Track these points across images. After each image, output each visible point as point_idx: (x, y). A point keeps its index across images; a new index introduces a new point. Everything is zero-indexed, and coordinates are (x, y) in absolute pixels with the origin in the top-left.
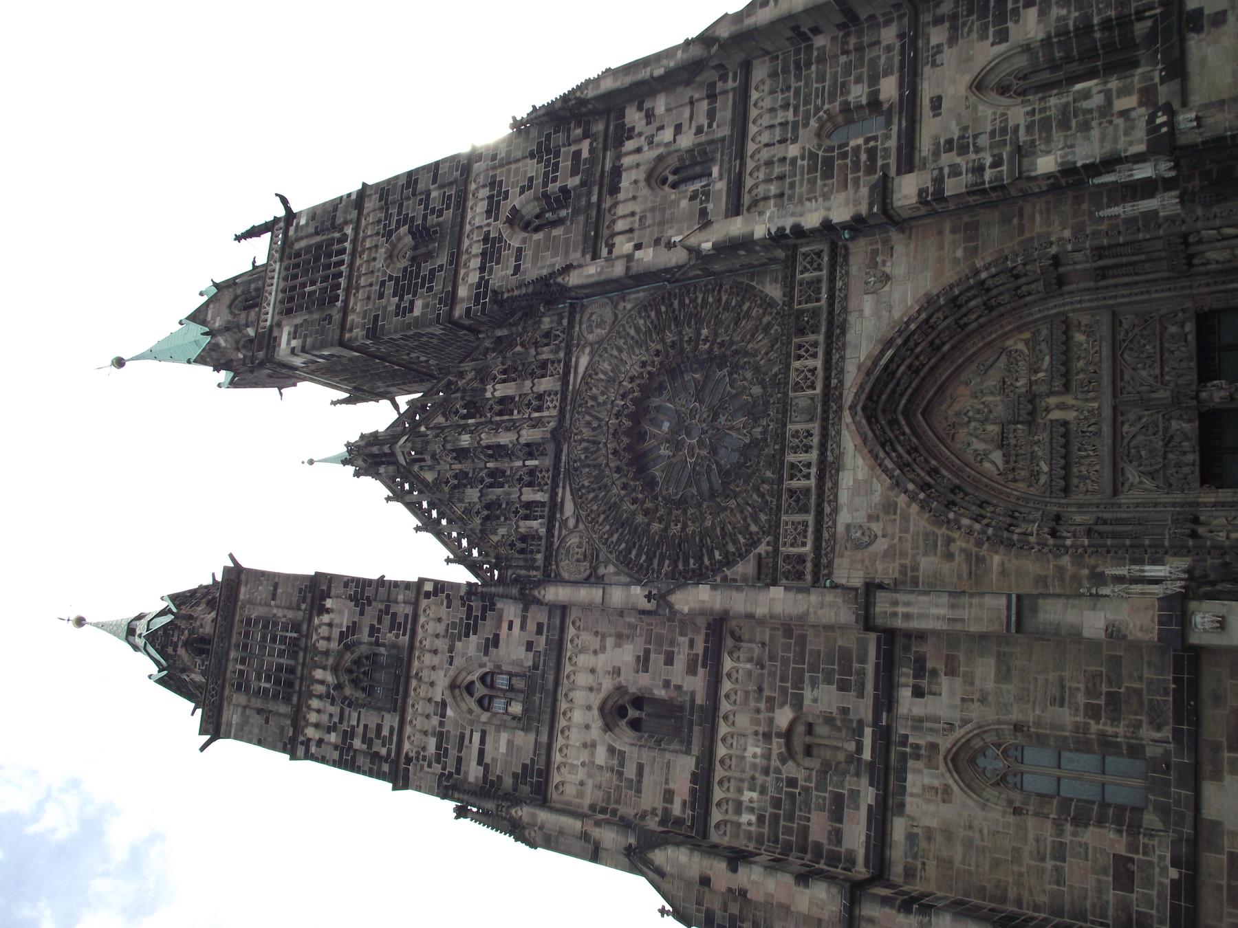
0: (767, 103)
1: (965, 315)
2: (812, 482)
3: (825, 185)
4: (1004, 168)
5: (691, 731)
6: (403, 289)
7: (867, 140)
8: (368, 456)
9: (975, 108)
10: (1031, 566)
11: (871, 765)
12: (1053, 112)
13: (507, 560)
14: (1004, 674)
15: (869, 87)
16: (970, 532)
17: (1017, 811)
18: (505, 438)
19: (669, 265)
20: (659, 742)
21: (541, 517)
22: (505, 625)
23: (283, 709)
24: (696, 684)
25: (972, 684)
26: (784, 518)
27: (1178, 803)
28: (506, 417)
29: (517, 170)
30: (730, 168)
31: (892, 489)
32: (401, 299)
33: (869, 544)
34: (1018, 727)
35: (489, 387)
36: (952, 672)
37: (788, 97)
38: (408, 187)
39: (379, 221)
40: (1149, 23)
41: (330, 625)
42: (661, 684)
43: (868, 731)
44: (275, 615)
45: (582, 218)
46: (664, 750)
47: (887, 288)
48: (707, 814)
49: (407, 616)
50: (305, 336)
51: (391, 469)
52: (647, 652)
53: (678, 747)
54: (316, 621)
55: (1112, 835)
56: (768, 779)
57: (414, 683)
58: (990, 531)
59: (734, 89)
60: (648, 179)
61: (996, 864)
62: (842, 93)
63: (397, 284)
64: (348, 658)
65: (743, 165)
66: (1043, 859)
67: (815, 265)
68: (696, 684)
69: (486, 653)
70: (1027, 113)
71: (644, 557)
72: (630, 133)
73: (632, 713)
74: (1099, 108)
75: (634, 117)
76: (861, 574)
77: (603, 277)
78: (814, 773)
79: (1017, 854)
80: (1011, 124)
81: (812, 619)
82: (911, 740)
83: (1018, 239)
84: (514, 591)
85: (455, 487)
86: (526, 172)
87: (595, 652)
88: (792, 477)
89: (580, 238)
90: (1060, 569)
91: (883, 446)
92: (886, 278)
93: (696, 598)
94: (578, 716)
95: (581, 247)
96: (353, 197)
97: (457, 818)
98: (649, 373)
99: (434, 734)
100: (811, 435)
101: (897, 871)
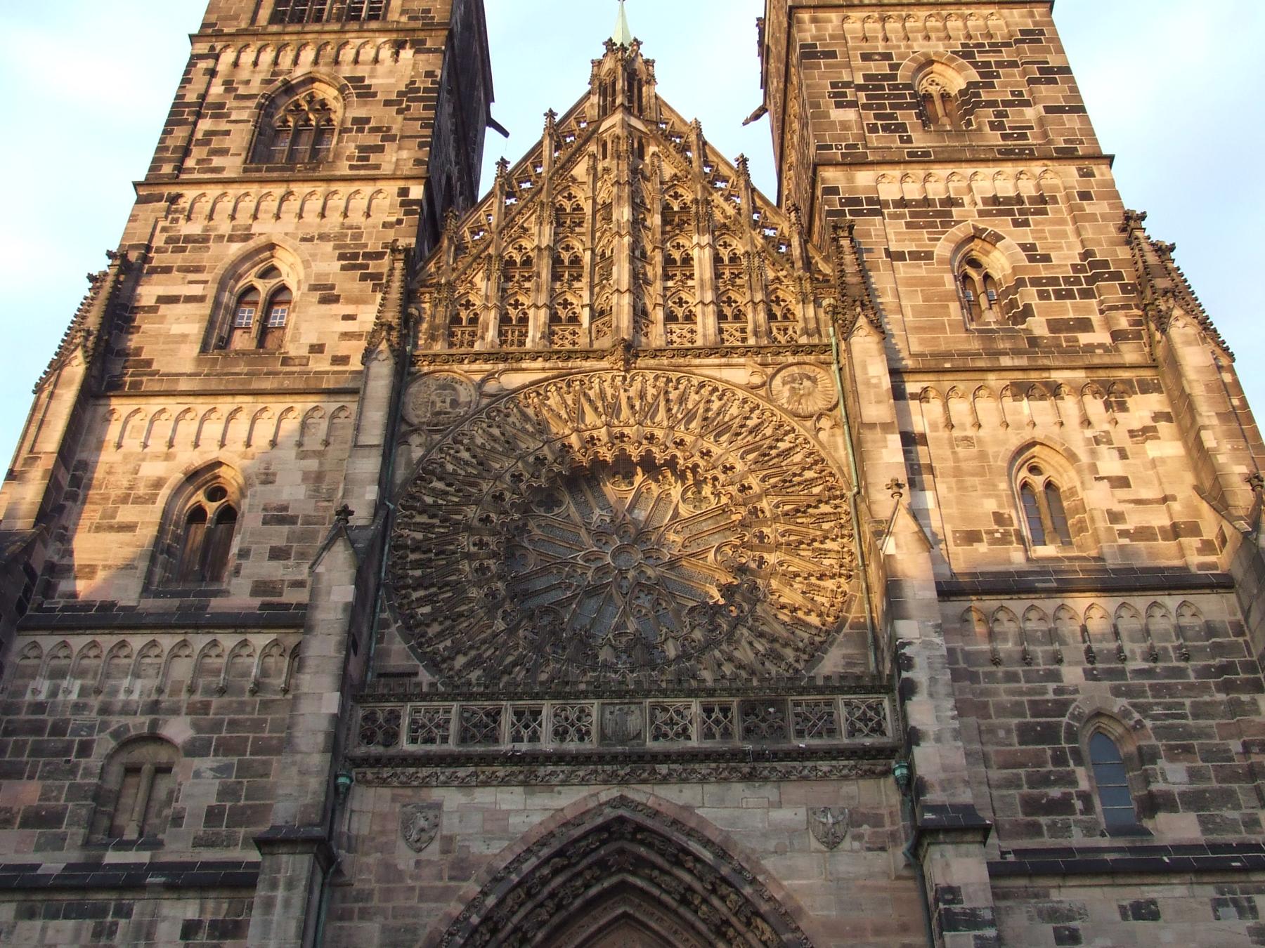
0: (1160, 623)
2: (505, 746)
3: (1008, 731)
5: (174, 595)
6: (876, 88)
7: (1085, 797)
11: (97, 865)
15: (1182, 794)
19: (872, 490)
21: (503, 343)
22: (349, 309)
24: (238, 595)
26: (455, 706)
29: (1064, 235)
31: (489, 871)
32: (860, 88)
35: (706, 239)
38: (1041, 70)
42: (246, 545)
45: (976, 345)
47: (814, 844)
48: (53, 628)
53: (156, 579)
54: (381, 39)
56: (94, 714)
62: (1170, 748)
63: (885, 77)
67: (859, 725)
68: (238, 595)
69: (314, 288)
71: (429, 500)
75: (1143, 408)
76: (365, 831)
77: (861, 388)
78: (95, 780)
82: (122, 922)
84: (392, 316)
86: (1061, 248)
87: (300, 444)
88: (519, 714)
89: (943, 348)
91: (560, 853)
92: (832, 842)
93: (337, 583)
95: (927, 350)
99: (206, 229)
100: (581, 739)
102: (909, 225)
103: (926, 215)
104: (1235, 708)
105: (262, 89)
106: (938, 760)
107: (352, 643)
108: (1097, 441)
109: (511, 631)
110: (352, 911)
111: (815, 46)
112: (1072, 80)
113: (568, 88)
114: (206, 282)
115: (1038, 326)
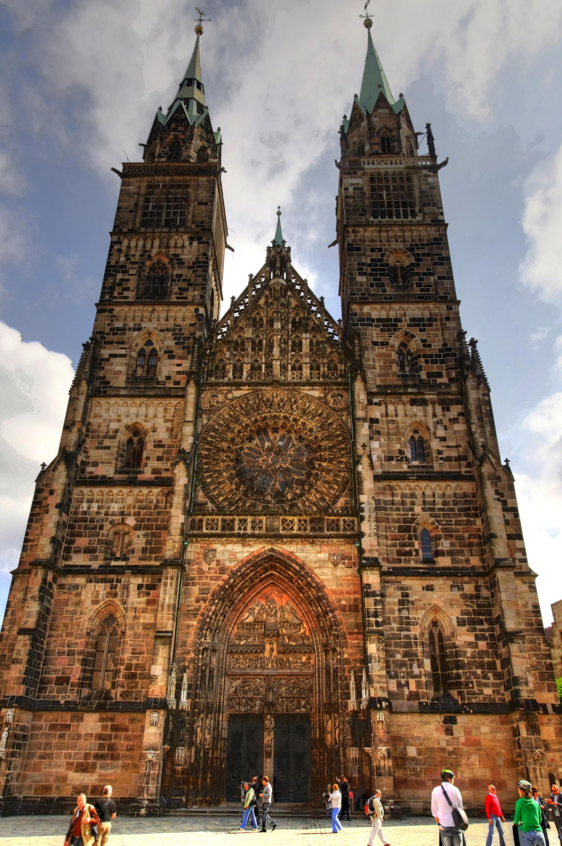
2: (236, 531)
4: (375, 628)
5: (126, 473)
7: (417, 551)
9: (423, 609)
11: (108, 566)
12: (414, 649)
14: (146, 627)
16: (209, 611)
17: (88, 634)
18: (276, 351)
20: (122, 456)
21: (234, 378)
22: (179, 362)
23: (138, 221)
24: (147, 474)
25: (143, 612)
27: (91, 703)
29: (438, 335)
32: (369, 265)
34: (123, 633)
35: (308, 335)
36: (148, 602)
38: (440, 259)
39: (420, 240)
40: (456, 697)
41: (183, 247)
43: (124, 563)
44: (189, 205)
45: (400, 383)
46: (117, 460)
47: (330, 565)
49: (186, 298)
55: (78, 676)
57: (150, 309)
58: (208, 620)
59: (460, 472)
61: (66, 626)
64: (166, 261)
65: (414, 481)
66: (68, 646)
68: (147, 474)
69: (166, 352)
71: (209, 439)
72: (446, 409)
73: (136, 439)
75: (455, 410)
76: (192, 558)
77: (357, 404)
79: (70, 635)
80: (411, 627)
84: (194, 368)
87: (165, 417)
88: (240, 521)
89: (388, 383)
90: (188, 653)
92: (335, 565)
94: (133, 410)
96: (440, 218)
97: (83, 345)
99: (125, 325)
101: (62, 580)
102: (381, 330)
103: (387, 326)
104: (468, 523)
108: (438, 423)
109: (237, 489)
111: (352, 245)
112: (450, 264)
115: (423, 375)
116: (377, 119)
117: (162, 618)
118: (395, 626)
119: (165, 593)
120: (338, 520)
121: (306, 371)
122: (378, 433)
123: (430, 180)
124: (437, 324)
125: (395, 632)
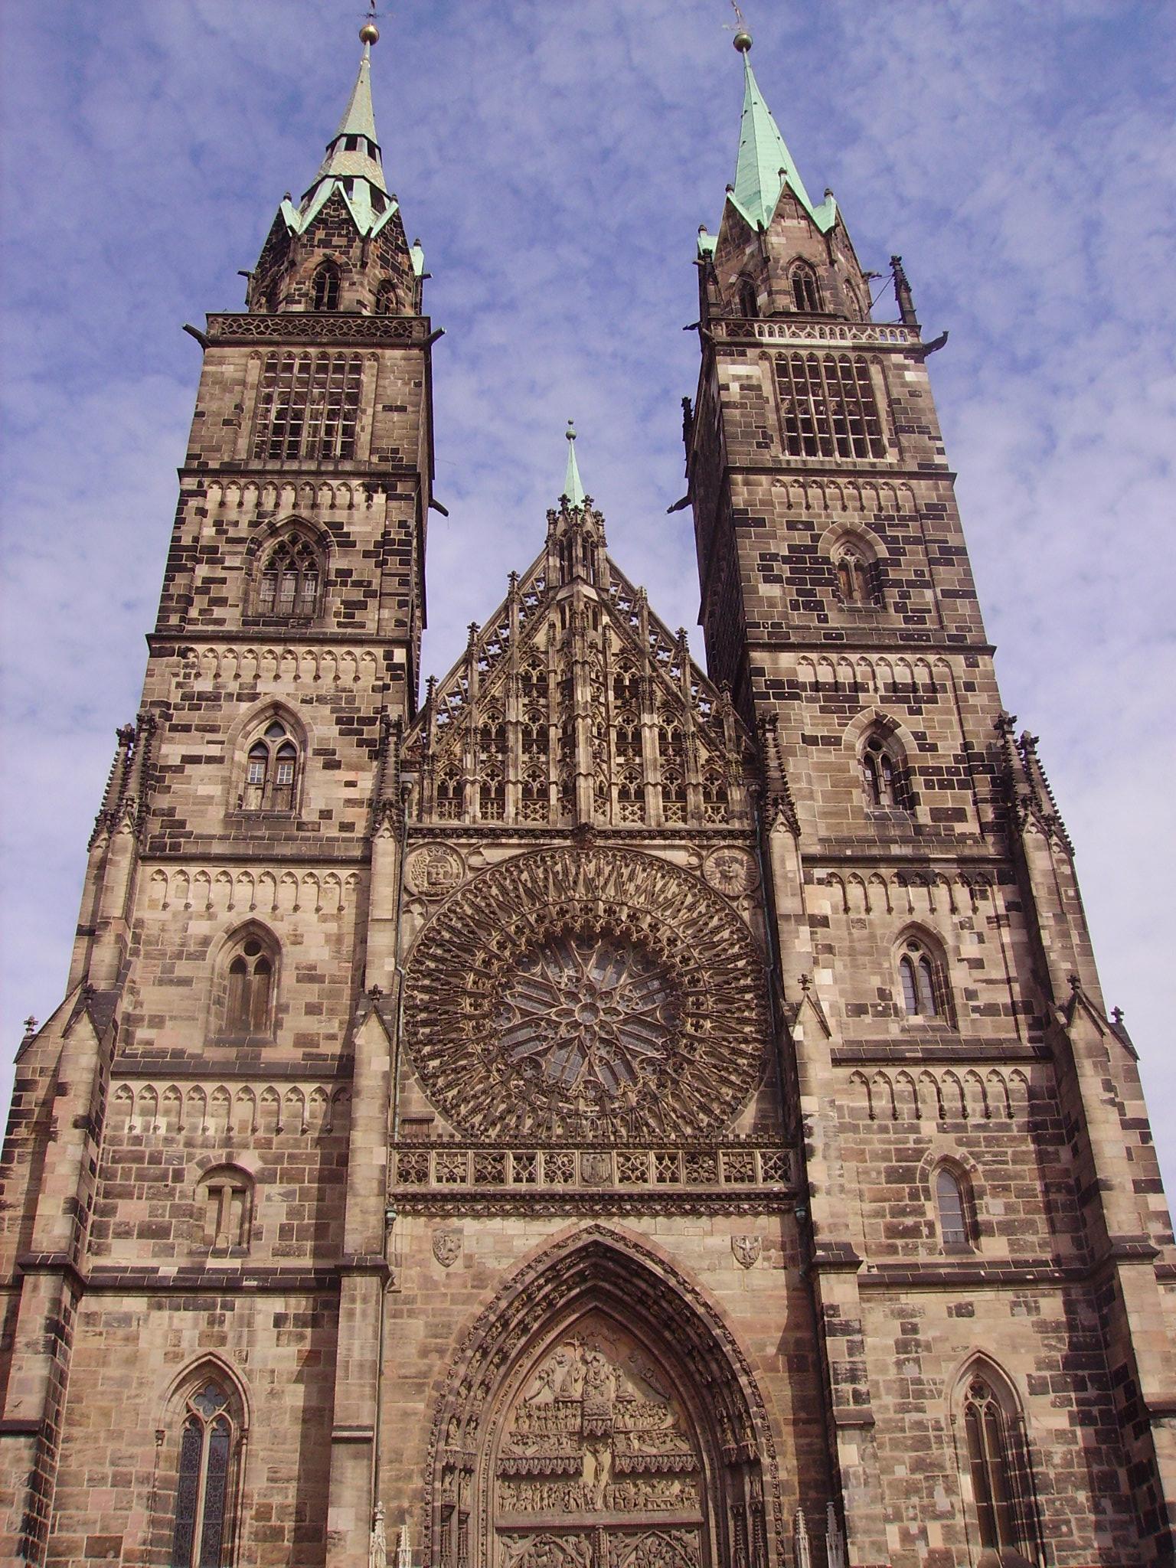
1: (703, 1358)
2: (510, 1186)
3: (879, 1173)
4: (852, 1406)
5: (232, 1044)
7: (931, 1225)
8: (573, 539)
10: (413, 1444)
11: (201, 1269)
13: (432, 771)
16: (450, 1375)
18: (583, 755)
20: (219, 1002)
21: (484, 816)
22: (350, 776)
23: (243, 443)
24: (283, 1051)
28: (613, 749)
30: (915, 1043)
32: (786, 560)
33: (436, 1255)
37: (999, 1116)
41: (351, 506)
44: (364, 411)
45: (872, 832)
47: (737, 1264)
48: (138, 1075)
49: (362, 626)
50: (743, 406)
51: (554, 577)
52: (320, 979)
54: (355, 483)
56: (181, 1146)
60: (914, 925)
61: (105, 1414)
62: (994, 1187)
65: (916, 1062)
66: (113, 1463)
69: (318, 752)
70: (937, 1422)
71: (432, 965)
73: (252, 961)
74: (934, 1505)
76: (406, 1250)
77: (778, 881)
78: (190, 1202)
79: (116, 1435)
81: (350, 1201)
82: (228, 1314)
83: (781, 1418)
84: (389, 794)
85: (527, 678)
87: (318, 910)
89: (846, 834)
90: (409, 1477)
91: (552, 1268)
94: (243, 891)
96: (938, 459)
98: (662, 950)
99: (216, 687)
100: (566, 1181)
102: (823, 710)
105: (250, 532)
106: (827, 1209)
107: (388, 1102)
110: (401, 1311)
112: (967, 562)
113: (525, 548)
114: (222, 743)
116: (783, 240)
117: (347, 1394)
118: (890, 1400)
119: (351, 1337)
120: (750, 1154)
121: (654, 801)
122: (829, 949)
123: (909, 376)
124: (946, 699)
125: (891, 1415)
